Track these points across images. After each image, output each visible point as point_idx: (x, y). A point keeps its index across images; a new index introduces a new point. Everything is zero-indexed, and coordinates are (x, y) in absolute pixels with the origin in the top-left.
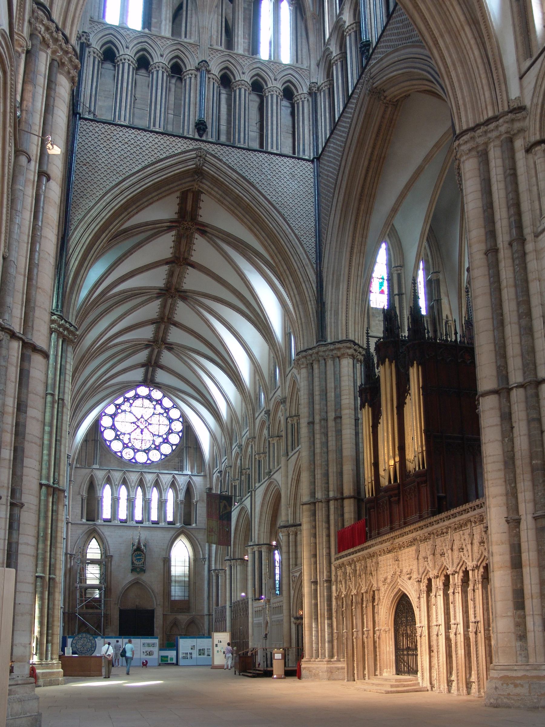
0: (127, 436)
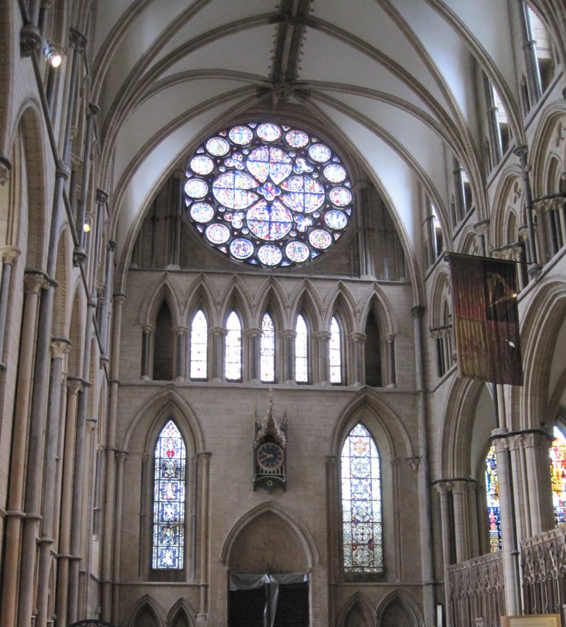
0: (240, 216)
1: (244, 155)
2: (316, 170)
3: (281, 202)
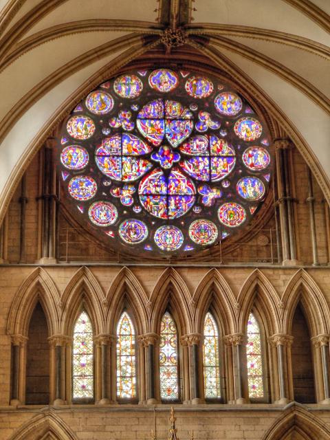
1: (132, 111)
2: (223, 127)
3: (182, 170)
